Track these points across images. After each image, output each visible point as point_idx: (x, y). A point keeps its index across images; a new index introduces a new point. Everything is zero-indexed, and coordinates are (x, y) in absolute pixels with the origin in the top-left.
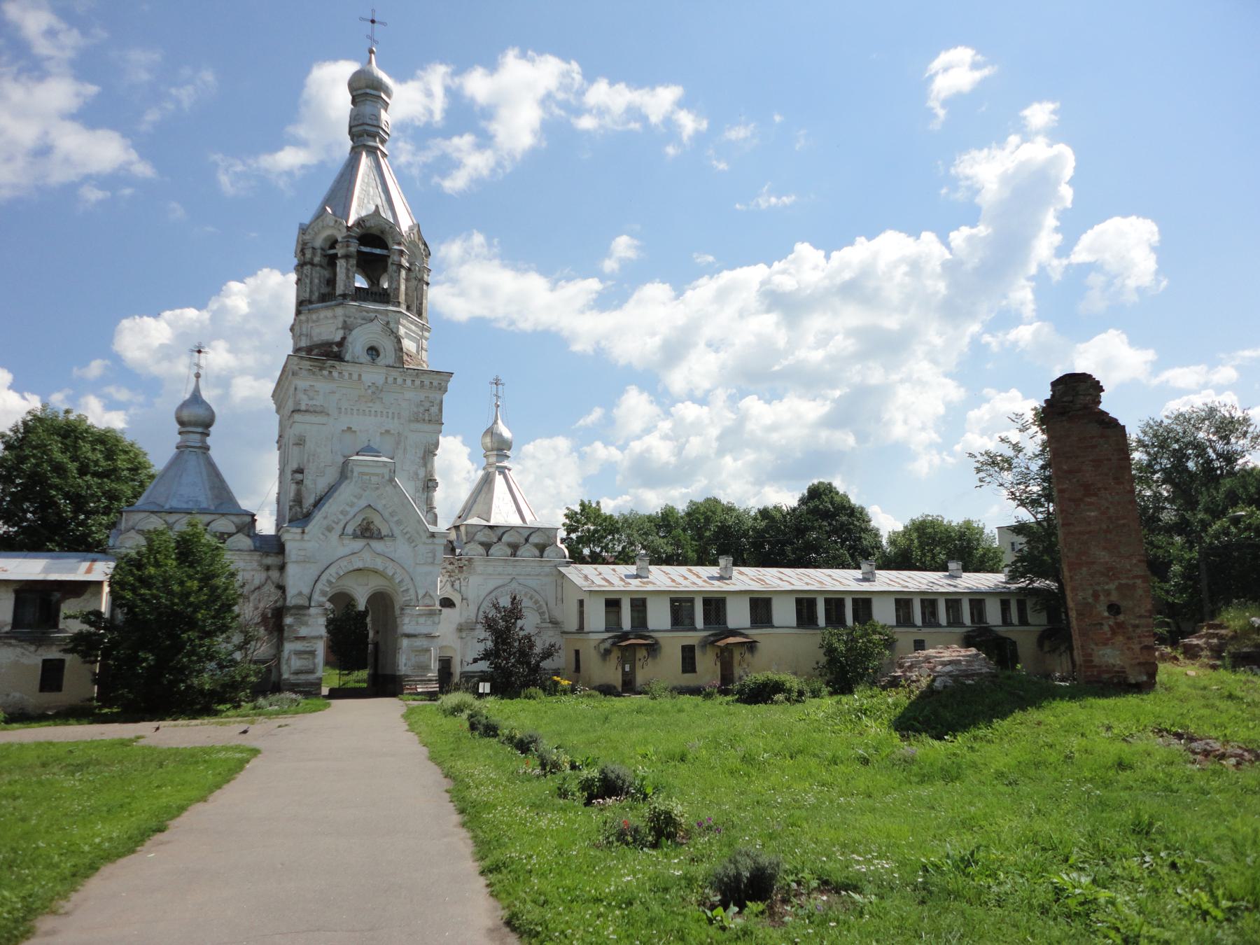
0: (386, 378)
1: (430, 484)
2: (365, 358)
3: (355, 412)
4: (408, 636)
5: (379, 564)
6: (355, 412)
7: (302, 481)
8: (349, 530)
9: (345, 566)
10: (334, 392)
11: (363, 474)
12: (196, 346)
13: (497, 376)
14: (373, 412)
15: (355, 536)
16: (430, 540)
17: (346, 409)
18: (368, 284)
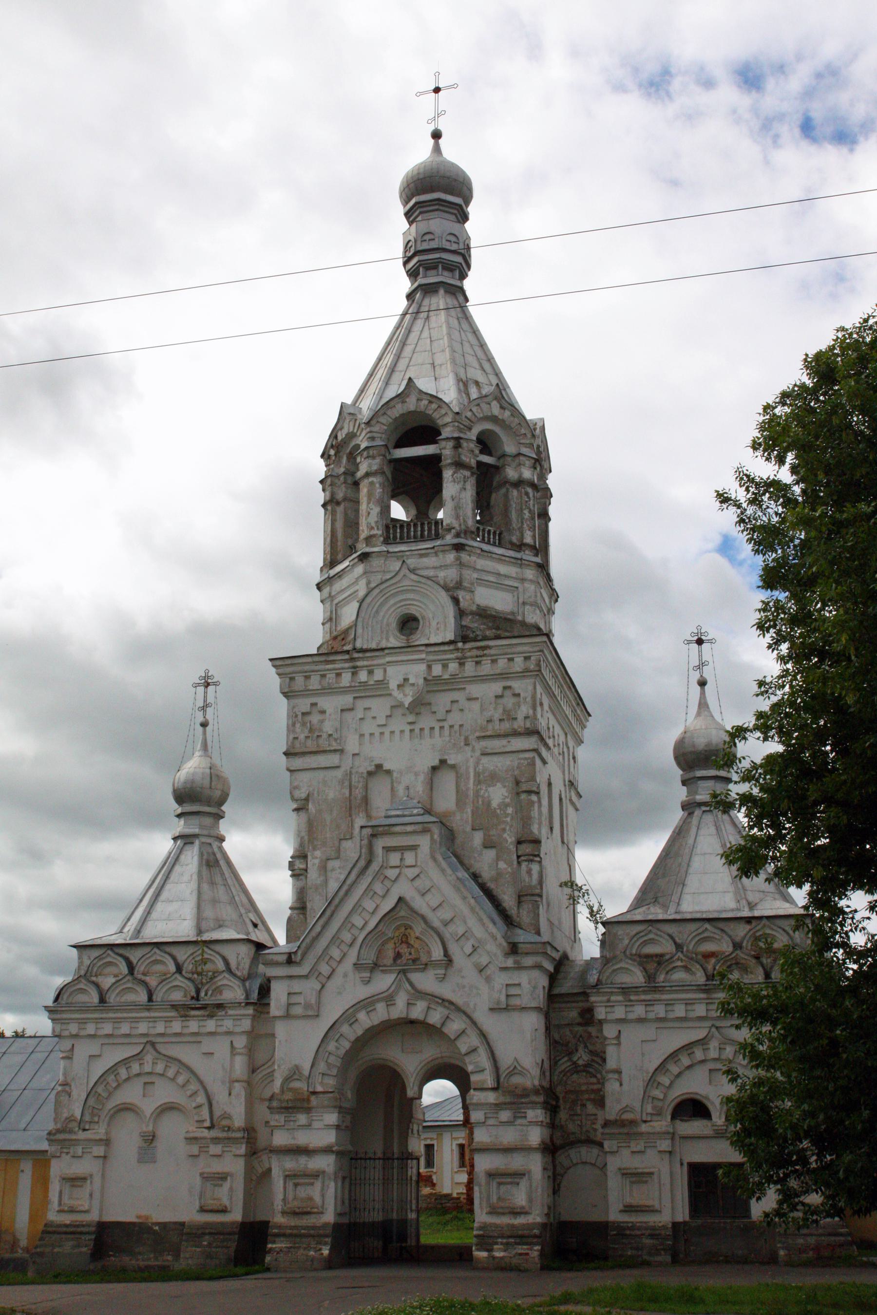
0: (429, 667)
1: (526, 848)
2: (394, 641)
3: (387, 734)
4: (485, 1150)
5: (417, 1012)
6: (387, 734)
7: (306, 870)
8: (369, 957)
9: (365, 1021)
10: (351, 709)
11: (388, 849)
12: (200, 678)
13: (699, 627)
14: (417, 731)
15: (375, 966)
16: (510, 962)
17: (372, 734)
18: (407, 512)
